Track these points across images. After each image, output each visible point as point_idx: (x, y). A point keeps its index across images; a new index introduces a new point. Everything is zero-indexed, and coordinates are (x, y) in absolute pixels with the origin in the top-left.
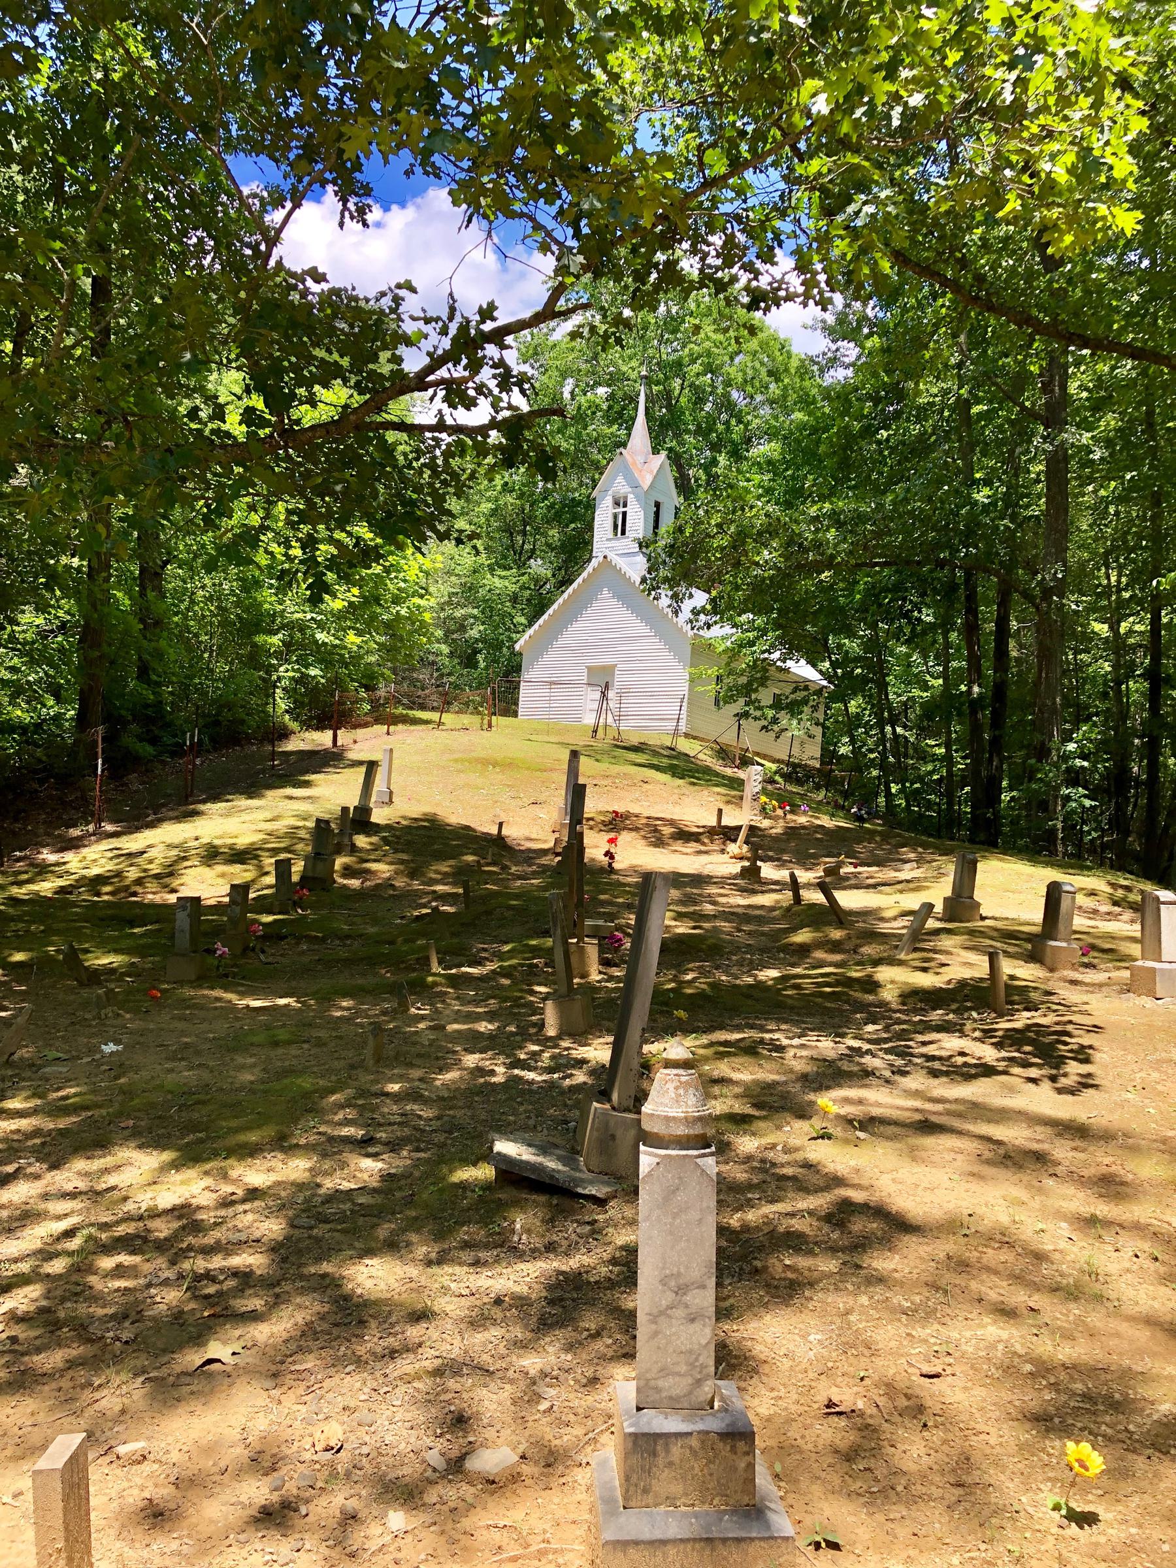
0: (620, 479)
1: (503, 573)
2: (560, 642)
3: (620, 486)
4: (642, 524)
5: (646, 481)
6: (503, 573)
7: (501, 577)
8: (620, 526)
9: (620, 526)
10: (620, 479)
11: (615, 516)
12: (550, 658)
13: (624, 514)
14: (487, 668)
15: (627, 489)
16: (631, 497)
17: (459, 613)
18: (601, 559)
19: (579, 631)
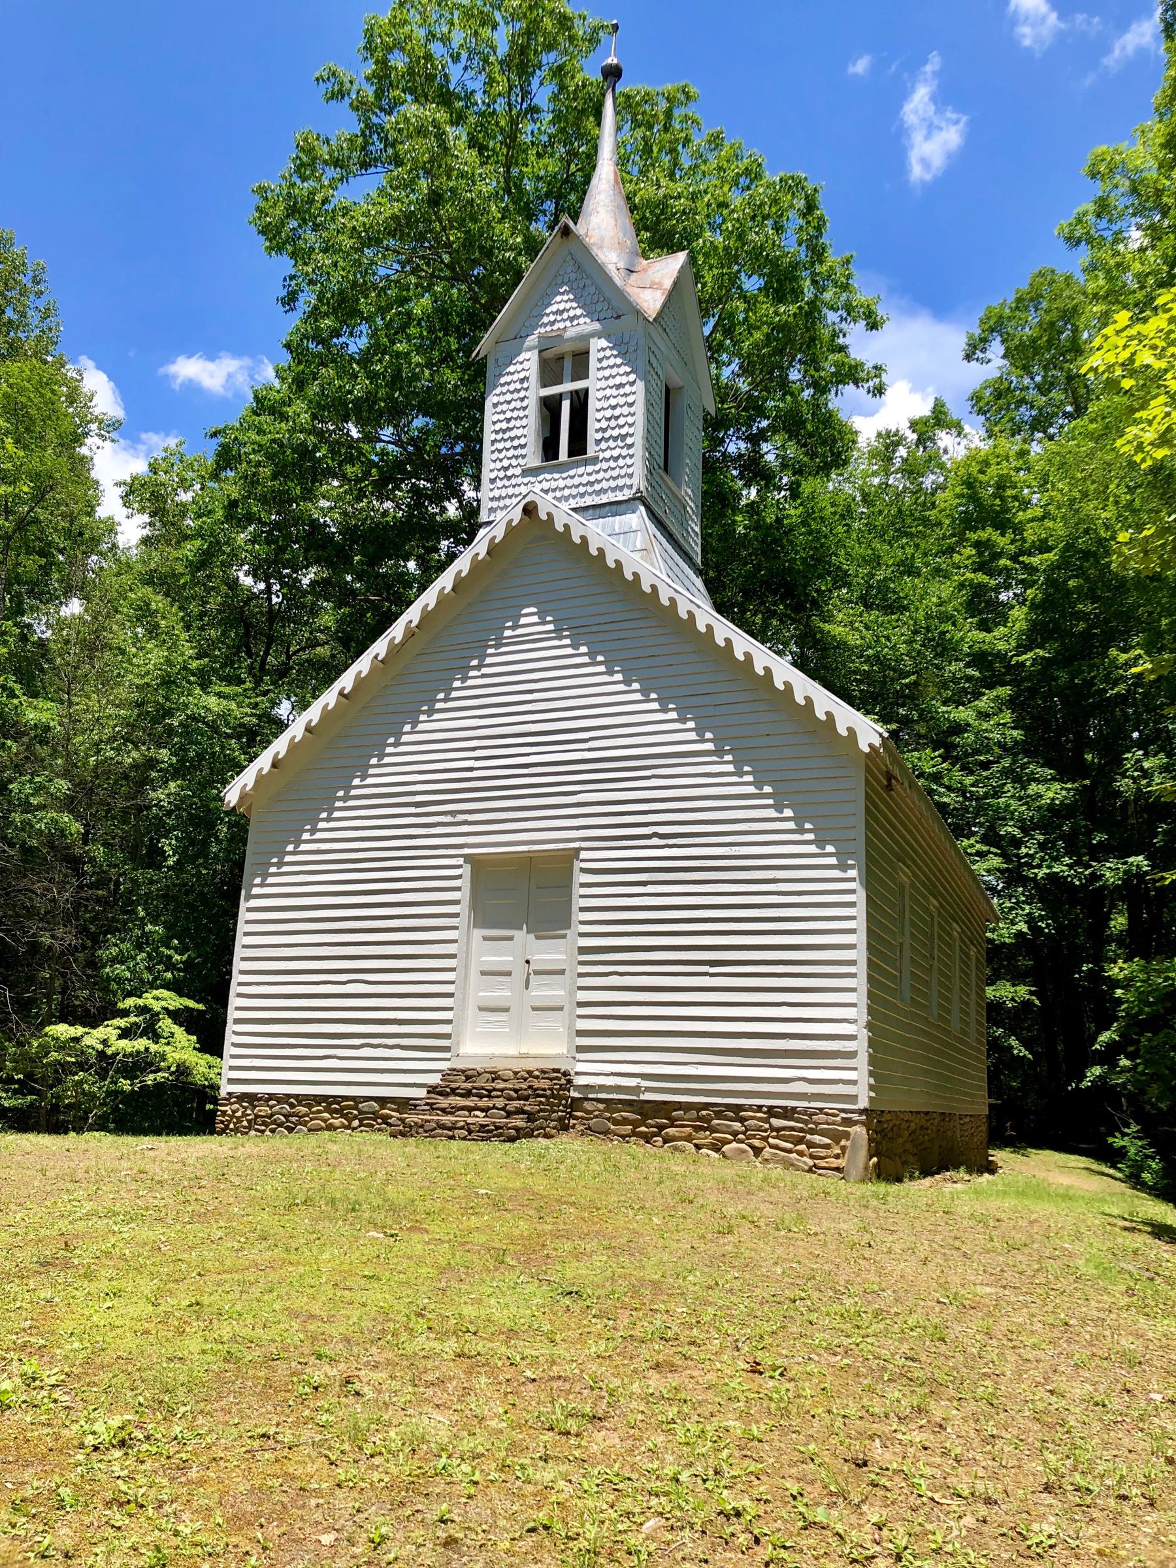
0: (562, 302)
1: (227, 690)
2: (377, 778)
3: (565, 318)
4: (640, 419)
5: (651, 302)
6: (227, 690)
7: (219, 695)
8: (565, 431)
9: (565, 431)
10: (562, 302)
11: (550, 407)
12: (338, 830)
13: (580, 402)
14: (179, 866)
15: (587, 325)
16: (597, 345)
17: (134, 755)
18: (517, 515)
19: (433, 746)
